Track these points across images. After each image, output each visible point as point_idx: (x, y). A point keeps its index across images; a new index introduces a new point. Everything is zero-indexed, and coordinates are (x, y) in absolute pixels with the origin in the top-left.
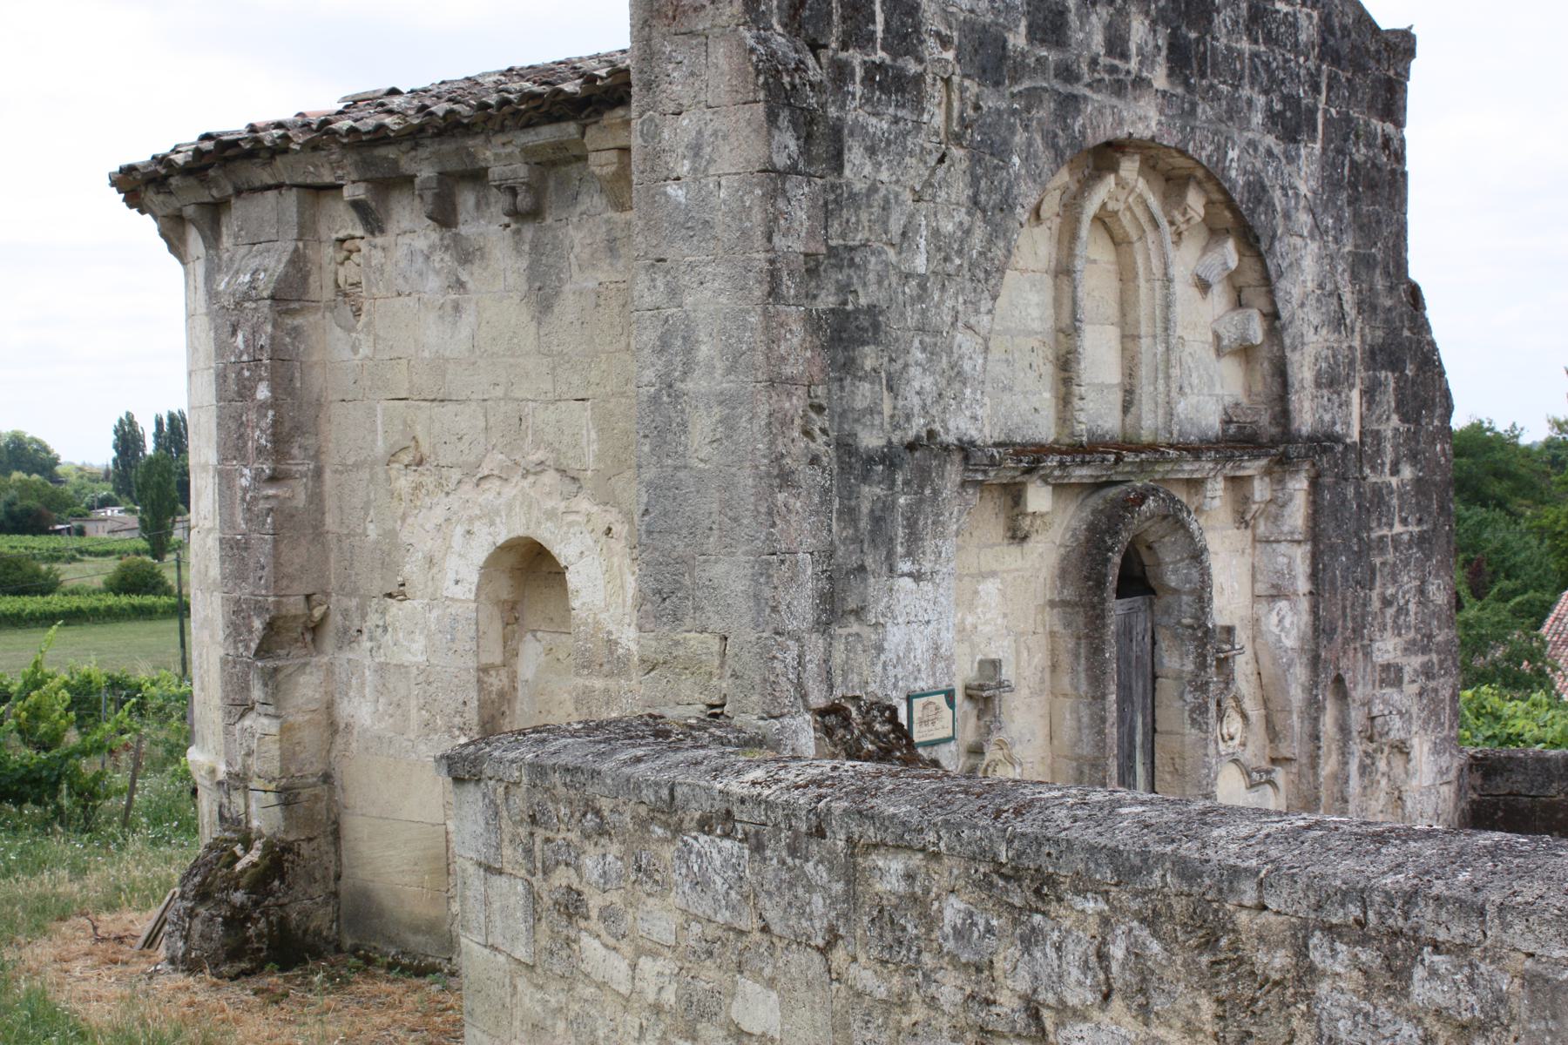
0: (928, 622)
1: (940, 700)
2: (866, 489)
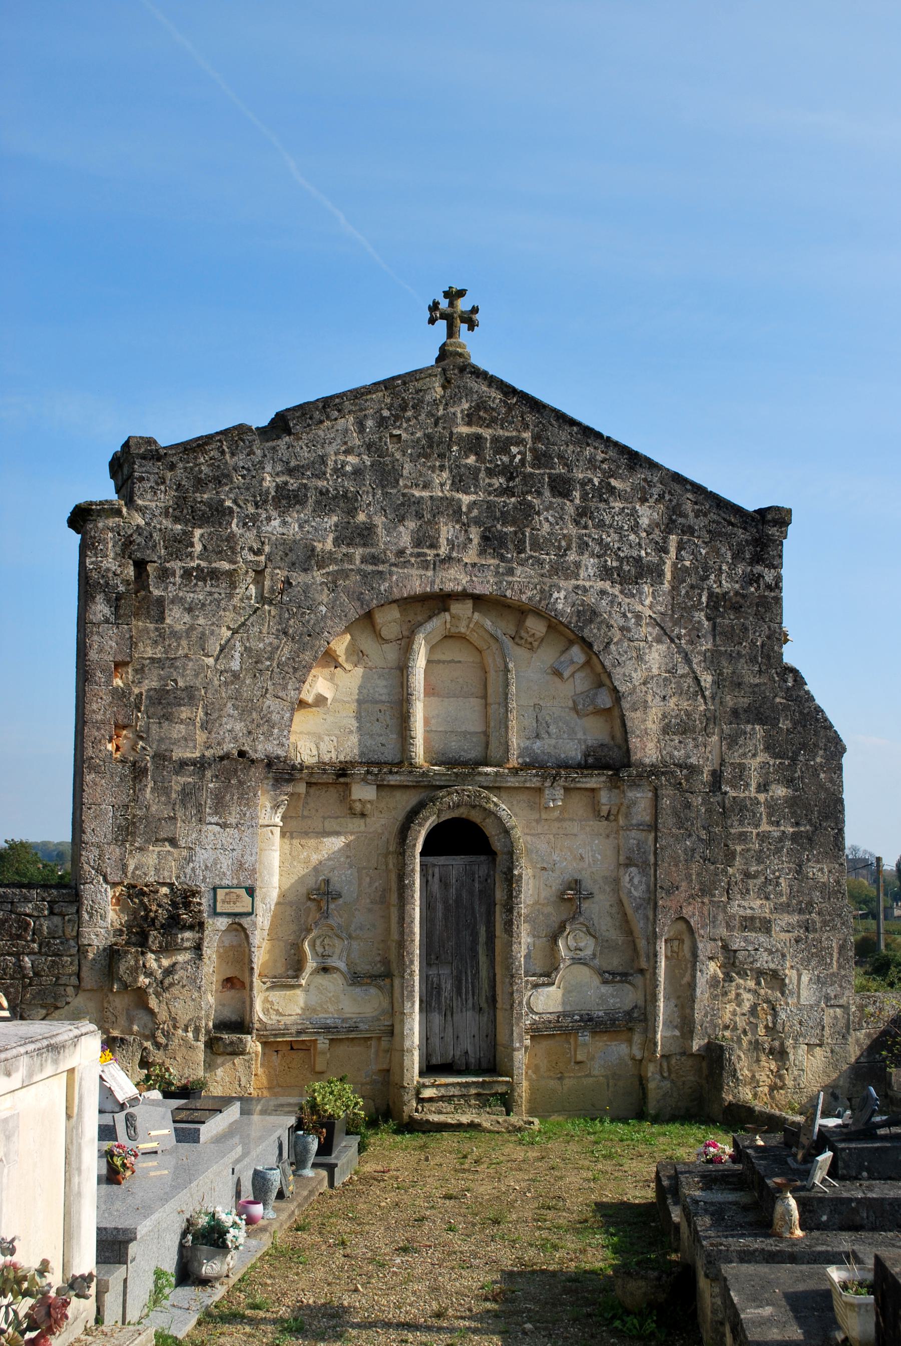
0: (233, 850)
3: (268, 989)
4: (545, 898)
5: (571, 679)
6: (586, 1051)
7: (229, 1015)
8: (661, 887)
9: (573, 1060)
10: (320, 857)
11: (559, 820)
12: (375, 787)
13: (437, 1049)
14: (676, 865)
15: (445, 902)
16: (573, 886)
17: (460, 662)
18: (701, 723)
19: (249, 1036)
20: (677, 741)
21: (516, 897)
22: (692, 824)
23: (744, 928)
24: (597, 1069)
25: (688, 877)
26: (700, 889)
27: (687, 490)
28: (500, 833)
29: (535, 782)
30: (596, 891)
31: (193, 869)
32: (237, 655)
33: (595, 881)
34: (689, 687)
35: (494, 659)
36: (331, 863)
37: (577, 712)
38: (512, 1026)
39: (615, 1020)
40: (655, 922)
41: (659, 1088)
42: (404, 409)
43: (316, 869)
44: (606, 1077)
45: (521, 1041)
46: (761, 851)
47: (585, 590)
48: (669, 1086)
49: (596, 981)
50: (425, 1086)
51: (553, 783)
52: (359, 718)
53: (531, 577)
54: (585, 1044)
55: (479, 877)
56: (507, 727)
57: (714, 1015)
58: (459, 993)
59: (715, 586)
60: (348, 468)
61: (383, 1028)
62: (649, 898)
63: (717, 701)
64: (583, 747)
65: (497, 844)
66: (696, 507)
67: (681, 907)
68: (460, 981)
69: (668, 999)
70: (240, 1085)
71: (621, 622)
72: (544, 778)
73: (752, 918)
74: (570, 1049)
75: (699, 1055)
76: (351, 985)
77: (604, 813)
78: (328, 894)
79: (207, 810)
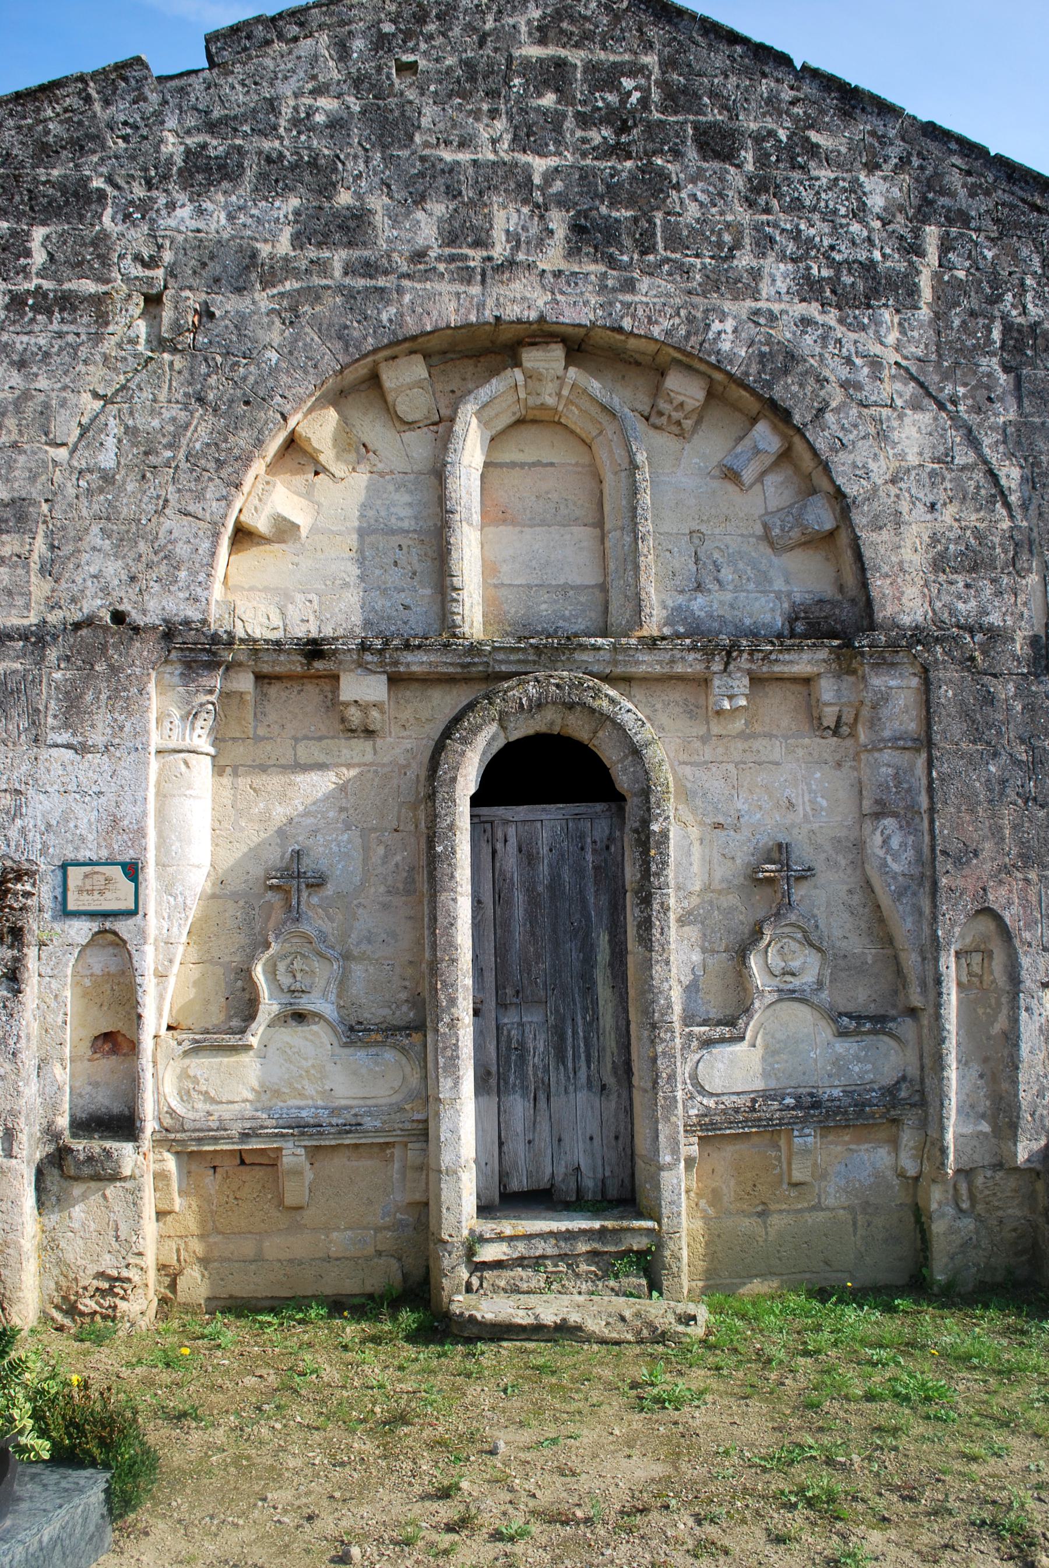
3: (186, 1054)
4: (722, 881)
5: (758, 487)
6: (809, 1163)
7: (107, 1102)
8: (944, 853)
9: (786, 1180)
10: (289, 811)
11: (742, 736)
12: (384, 677)
13: (521, 1163)
14: (972, 811)
15: (530, 890)
16: (775, 855)
17: (552, 464)
18: (1005, 552)
19: (128, 1147)
20: (961, 584)
21: (658, 875)
22: (999, 733)
24: (833, 1195)
25: (996, 832)
26: (1020, 855)
27: (951, 152)
28: (626, 757)
29: (691, 664)
30: (819, 866)
31: (23, 831)
32: (111, 442)
33: (818, 848)
34: (978, 487)
35: (611, 451)
36: (310, 820)
37: (771, 544)
38: (657, 1122)
39: (864, 1105)
40: (935, 918)
41: (951, 1231)
42: (421, 18)
43: (281, 832)
44: (851, 1209)
45: (675, 1151)
47: (772, 317)
48: (972, 1227)
49: (825, 1032)
50: (482, 1240)
51: (727, 664)
52: (361, 561)
53: (668, 295)
54: (806, 1151)
55: (594, 842)
56: (637, 567)
58: (561, 1058)
59: (1014, 313)
60: (319, 118)
61: (408, 1126)
62: (922, 875)
63: (1033, 511)
64: (786, 605)
65: (623, 781)
66: (970, 180)
67: (984, 889)
68: (562, 1038)
69: (966, 1064)
70: (117, 1237)
71: (844, 372)
72: (708, 653)
74: (779, 1159)
75: (1030, 1170)
76: (345, 1045)
77: (829, 721)
78: (299, 877)
79: (50, 720)
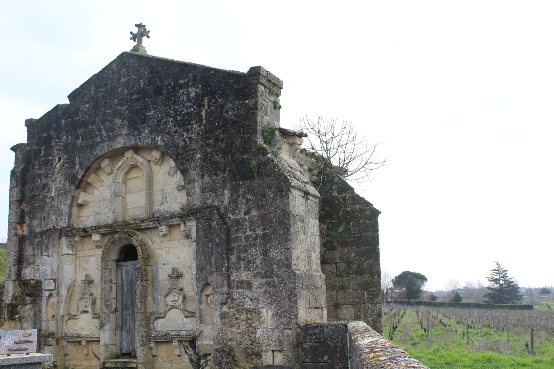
1: (52, 281)
2: (36, 240)
11: (169, 240)
17: (139, 177)
20: (208, 195)
23: (237, 287)
30: (185, 273)
46: (246, 246)
57: (223, 333)
64: (181, 205)
73: (242, 282)
